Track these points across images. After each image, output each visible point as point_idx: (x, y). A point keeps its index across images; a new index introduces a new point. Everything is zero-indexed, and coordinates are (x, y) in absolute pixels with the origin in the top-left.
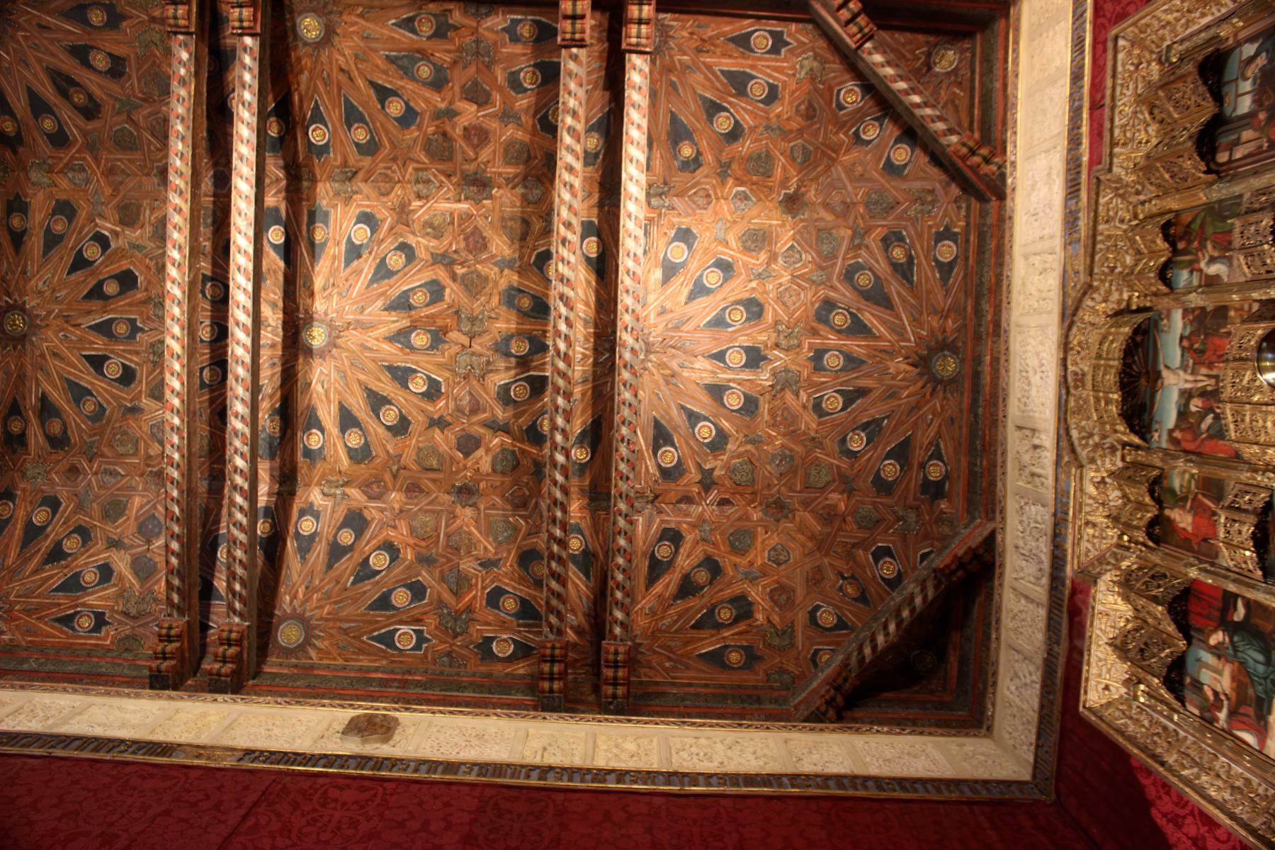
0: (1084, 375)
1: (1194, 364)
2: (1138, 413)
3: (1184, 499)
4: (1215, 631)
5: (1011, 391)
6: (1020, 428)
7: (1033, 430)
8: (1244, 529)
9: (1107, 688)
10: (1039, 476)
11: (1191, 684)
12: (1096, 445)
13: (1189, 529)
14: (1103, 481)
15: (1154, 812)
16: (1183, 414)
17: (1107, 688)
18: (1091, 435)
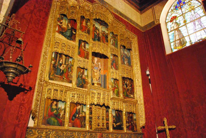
0: (102, 9)
2: (97, 20)
3: (87, 25)
4: (71, 26)
11: (62, 17)
13: (83, 24)
14: (89, 7)
18: (95, 7)
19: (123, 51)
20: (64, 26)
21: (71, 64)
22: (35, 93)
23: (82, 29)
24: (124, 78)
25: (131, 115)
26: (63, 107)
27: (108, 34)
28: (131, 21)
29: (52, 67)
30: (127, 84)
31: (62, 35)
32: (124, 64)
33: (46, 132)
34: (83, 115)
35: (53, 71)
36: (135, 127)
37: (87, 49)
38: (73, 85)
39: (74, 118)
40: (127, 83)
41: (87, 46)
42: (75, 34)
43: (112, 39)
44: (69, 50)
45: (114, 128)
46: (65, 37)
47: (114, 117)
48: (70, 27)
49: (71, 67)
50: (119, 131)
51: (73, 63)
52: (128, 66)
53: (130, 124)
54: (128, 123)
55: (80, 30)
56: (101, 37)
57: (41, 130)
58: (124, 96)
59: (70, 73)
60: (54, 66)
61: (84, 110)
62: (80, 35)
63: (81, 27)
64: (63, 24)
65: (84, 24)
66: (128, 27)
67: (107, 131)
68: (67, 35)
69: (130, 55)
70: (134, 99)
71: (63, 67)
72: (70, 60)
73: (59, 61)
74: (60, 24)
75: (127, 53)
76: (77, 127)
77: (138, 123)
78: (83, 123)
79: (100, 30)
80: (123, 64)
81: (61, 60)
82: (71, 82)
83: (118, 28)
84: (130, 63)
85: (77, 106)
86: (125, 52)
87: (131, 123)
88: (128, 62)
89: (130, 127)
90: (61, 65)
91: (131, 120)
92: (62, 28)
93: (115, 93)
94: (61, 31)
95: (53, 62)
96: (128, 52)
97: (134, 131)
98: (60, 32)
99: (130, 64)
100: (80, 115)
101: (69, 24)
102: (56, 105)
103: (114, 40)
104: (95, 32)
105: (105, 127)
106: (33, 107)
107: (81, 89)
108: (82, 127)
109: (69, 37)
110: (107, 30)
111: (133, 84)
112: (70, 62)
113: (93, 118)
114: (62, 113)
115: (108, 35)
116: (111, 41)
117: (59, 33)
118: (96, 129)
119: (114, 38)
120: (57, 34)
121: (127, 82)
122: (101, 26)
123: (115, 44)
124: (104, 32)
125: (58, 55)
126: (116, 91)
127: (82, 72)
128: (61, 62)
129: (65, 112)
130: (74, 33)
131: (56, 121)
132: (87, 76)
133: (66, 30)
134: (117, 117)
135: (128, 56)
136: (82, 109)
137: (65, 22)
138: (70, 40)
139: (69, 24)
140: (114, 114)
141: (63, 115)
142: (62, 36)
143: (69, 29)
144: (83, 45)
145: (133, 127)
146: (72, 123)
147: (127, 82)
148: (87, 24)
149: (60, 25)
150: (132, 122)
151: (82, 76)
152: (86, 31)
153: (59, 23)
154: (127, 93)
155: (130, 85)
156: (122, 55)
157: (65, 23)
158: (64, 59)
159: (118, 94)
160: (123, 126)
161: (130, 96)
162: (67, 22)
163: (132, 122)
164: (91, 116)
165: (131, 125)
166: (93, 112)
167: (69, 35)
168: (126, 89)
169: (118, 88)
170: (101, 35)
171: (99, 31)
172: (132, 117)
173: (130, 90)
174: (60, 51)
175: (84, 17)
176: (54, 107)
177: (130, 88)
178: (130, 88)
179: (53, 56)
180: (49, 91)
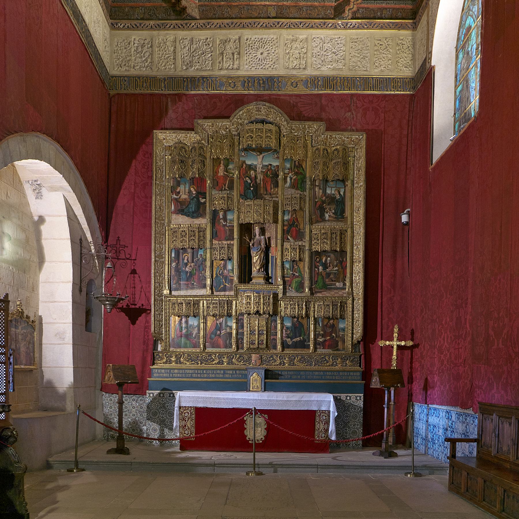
1: (264, 172)
2: (248, 149)
3: (227, 172)
4: (195, 190)
5: (255, 31)
6: (240, 38)
7: (239, 54)
8: (223, 205)
9: (164, 139)
10: (223, 59)
11: (178, 181)
12: (238, 122)
13: (219, 175)
14: (227, 128)
15: (134, 161)
16: (250, 167)
17: (164, 139)
19: (321, 191)
20: (184, 196)
21: (203, 258)
22: (153, 313)
23: (218, 185)
24: (315, 255)
25: (331, 321)
26: (196, 324)
27: (278, 166)
28: (366, 82)
29: (173, 273)
30: (328, 262)
31: (182, 214)
32: (324, 220)
33: (176, 356)
34: (228, 330)
35: (176, 277)
36: (340, 344)
37: (232, 220)
38: (208, 291)
39: (213, 336)
40: (326, 260)
41: (229, 217)
42: (205, 203)
43: (290, 174)
44: (194, 238)
45: (284, 346)
46: (188, 216)
47: (287, 328)
48: (194, 193)
49: (203, 263)
50: (299, 351)
51: (206, 256)
52: (334, 221)
53: (328, 338)
54: (323, 336)
55: (214, 188)
56: (262, 183)
57: (169, 354)
58: (311, 289)
59: (201, 273)
60: (178, 270)
61: (229, 324)
62: (216, 199)
63: (216, 182)
64: (181, 194)
65: (221, 173)
66: (350, 111)
67: (273, 351)
68: (191, 210)
69: (344, 192)
70: (344, 291)
71: (190, 266)
72: (201, 252)
73: (183, 259)
74: (176, 197)
75: (333, 192)
76: (218, 347)
77: (347, 335)
78: (228, 342)
79: (259, 170)
80: (321, 222)
81: (186, 258)
82: (204, 286)
83: (311, 134)
84: (343, 211)
85: (217, 320)
86: (328, 191)
87: (331, 335)
88: (333, 213)
89: (327, 343)
90: (186, 264)
91: (332, 331)
92: (180, 202)
93: (292, 288)
94: (179, 208)
95: (174, 264)
96: (340, 185)
97: (338, 350)
98: (179, 210)
99: (340, 214)
100: (223, 332)
101: (192, 189)
102: (187, 322)
103: (296, 174)
104: (247, 178)
105: (264, 346)
106: (153, 329)
107: (222, 293)
108: (226, 347)
109: (193, 213)
110: (278, 158)
111: (344, 259)
112: (201, 255)
113: (245, 333)
114: (195, 332)
115: (278, 171)
116: (288, 179)
117: (177, 214)
118: (248, 349)
119: (297, 167)
120: (174, 216)
121: (329, 259)
122: (261, 156)
123: (299, 184)
124: (270, 166)
125: (181, 251)
126: (296, 282)
127: (222, 265)
128: (186, 261)
129: (199, 330)
130: (203, 201)
131: (188, 342)
132: (233, 270)
133: (188, 201)
134: (295, 328)
135: (338, 197)
136: (226, 323)
137: (185, 188)
138: (197, 217)
139: (192, 189)
140: (288, 324)
141: (196, 334)
142: (182, 216)
143: (194, 197)
144: (221, 217)
145: (337, 342)
146: (210, 343)
147: (329, 259)
148: (227, 169)
149: (176, 199)
150: (333, 335)
151: (222, 273)
152: (225, 186)
153: (175, 196)
154: (324, 282)
155: (335, 264)
156: (316, 202)
157: (185, 191)
158: (190, 255)
159: (300, 287)
160: (309, 341)
161: (333, 287)
162: (187, 186)
163: (333, 335)
164: (240, 331)
165: (330, 339)
166: (245, 325)
167: (193, 210)
168: (324, 274)
169: (301, 276)
170: (260, 177)
171: (255, 171)
172: (333, 326)
173: (335, 273)
174: (180, 245)
175: (218, 158)
176: (184, 325)
177: (337, 268)
178: (337, 268)
179: (173, 255)
180: (174, 307)
